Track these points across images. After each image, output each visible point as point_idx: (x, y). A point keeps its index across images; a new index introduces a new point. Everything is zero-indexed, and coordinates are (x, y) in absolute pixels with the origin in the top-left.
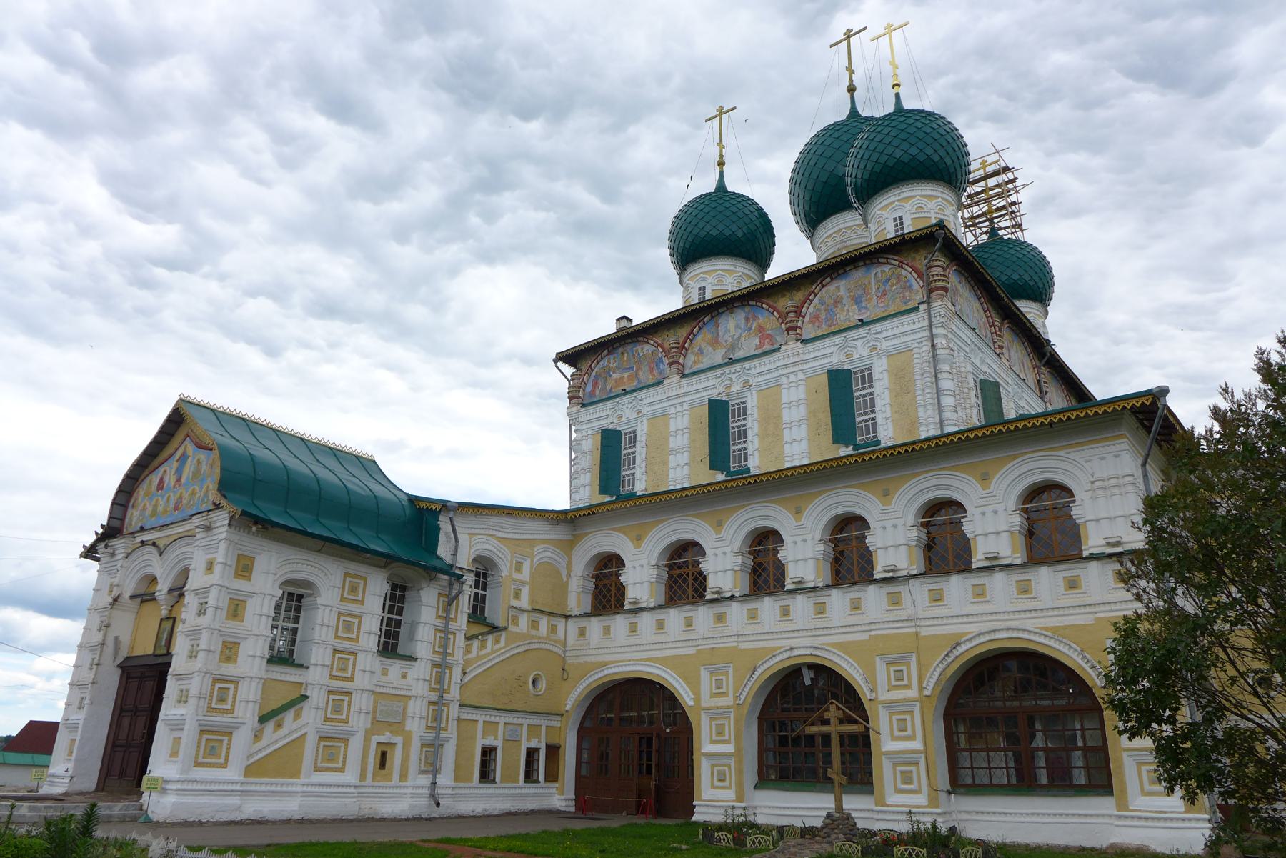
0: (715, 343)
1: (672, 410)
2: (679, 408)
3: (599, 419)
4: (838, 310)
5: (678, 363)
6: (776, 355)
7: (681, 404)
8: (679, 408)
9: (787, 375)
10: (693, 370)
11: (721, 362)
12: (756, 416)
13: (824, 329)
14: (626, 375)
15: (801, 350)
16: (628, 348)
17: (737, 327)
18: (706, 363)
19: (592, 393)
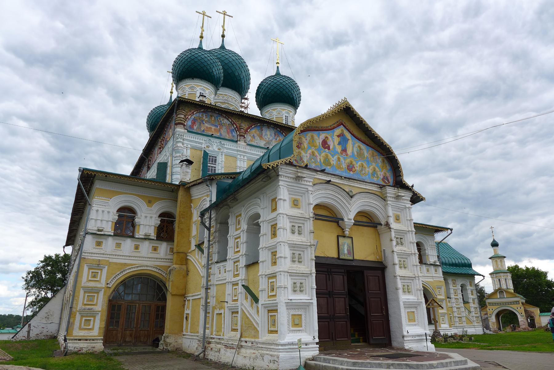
0: (261, 136)
1: (239, 157)
2: (242, 157)
3: (196, 142)
7: (244, 156)
10: (250, 143)
14: (213, 127)
16: (215, 115)
17: (271, 135)
19: (191, 127)
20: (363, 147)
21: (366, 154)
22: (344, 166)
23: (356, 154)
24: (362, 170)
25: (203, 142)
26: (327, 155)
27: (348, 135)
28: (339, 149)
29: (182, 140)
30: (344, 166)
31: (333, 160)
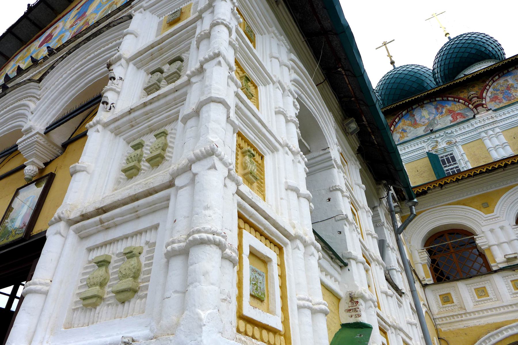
0: (415, 124)
4: (512, 91)
6: (473, 121)
9: (486, 132)
10: (401, 141)
11: (424, 134)
12: (467, 159)
13: (505, 102)
17: (430, 113)
18: (410, 136)
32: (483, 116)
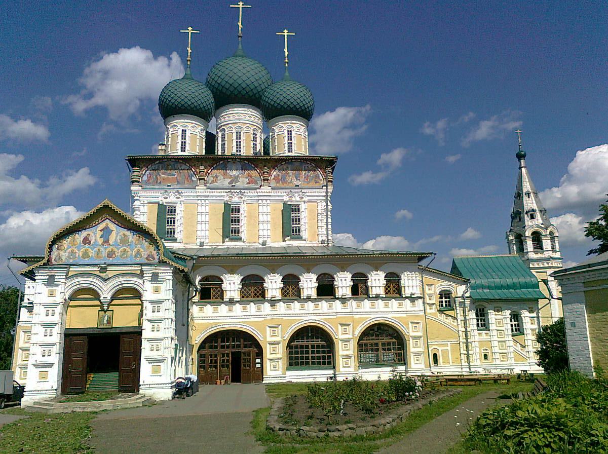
1: (199, 202)
5: (204, 179)
6: (258, 190)
8: (203, 201)
10: (213, 185)
15: (270, 191)
20: (128, 233)
21: (131, 239)
22: (104, 253)
23: (119, 241)
24: (123, 255)
25: (160, 194)
26: (86, 250)
27: (112, 226)
28: (100, 241)
29: (138, 198)
30: (104, 255)
31: (92, 253)
32: (266, 189)
